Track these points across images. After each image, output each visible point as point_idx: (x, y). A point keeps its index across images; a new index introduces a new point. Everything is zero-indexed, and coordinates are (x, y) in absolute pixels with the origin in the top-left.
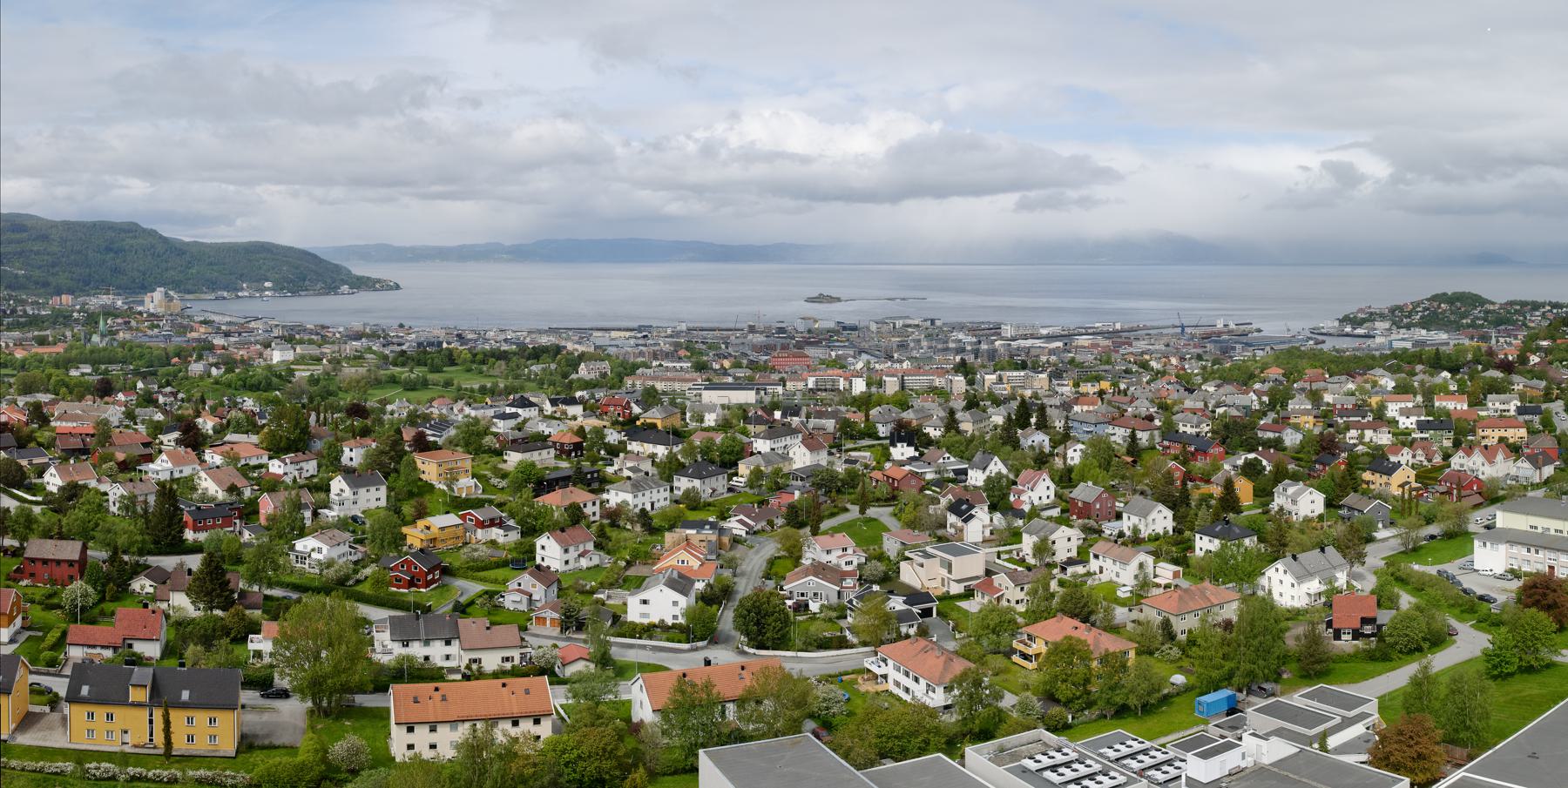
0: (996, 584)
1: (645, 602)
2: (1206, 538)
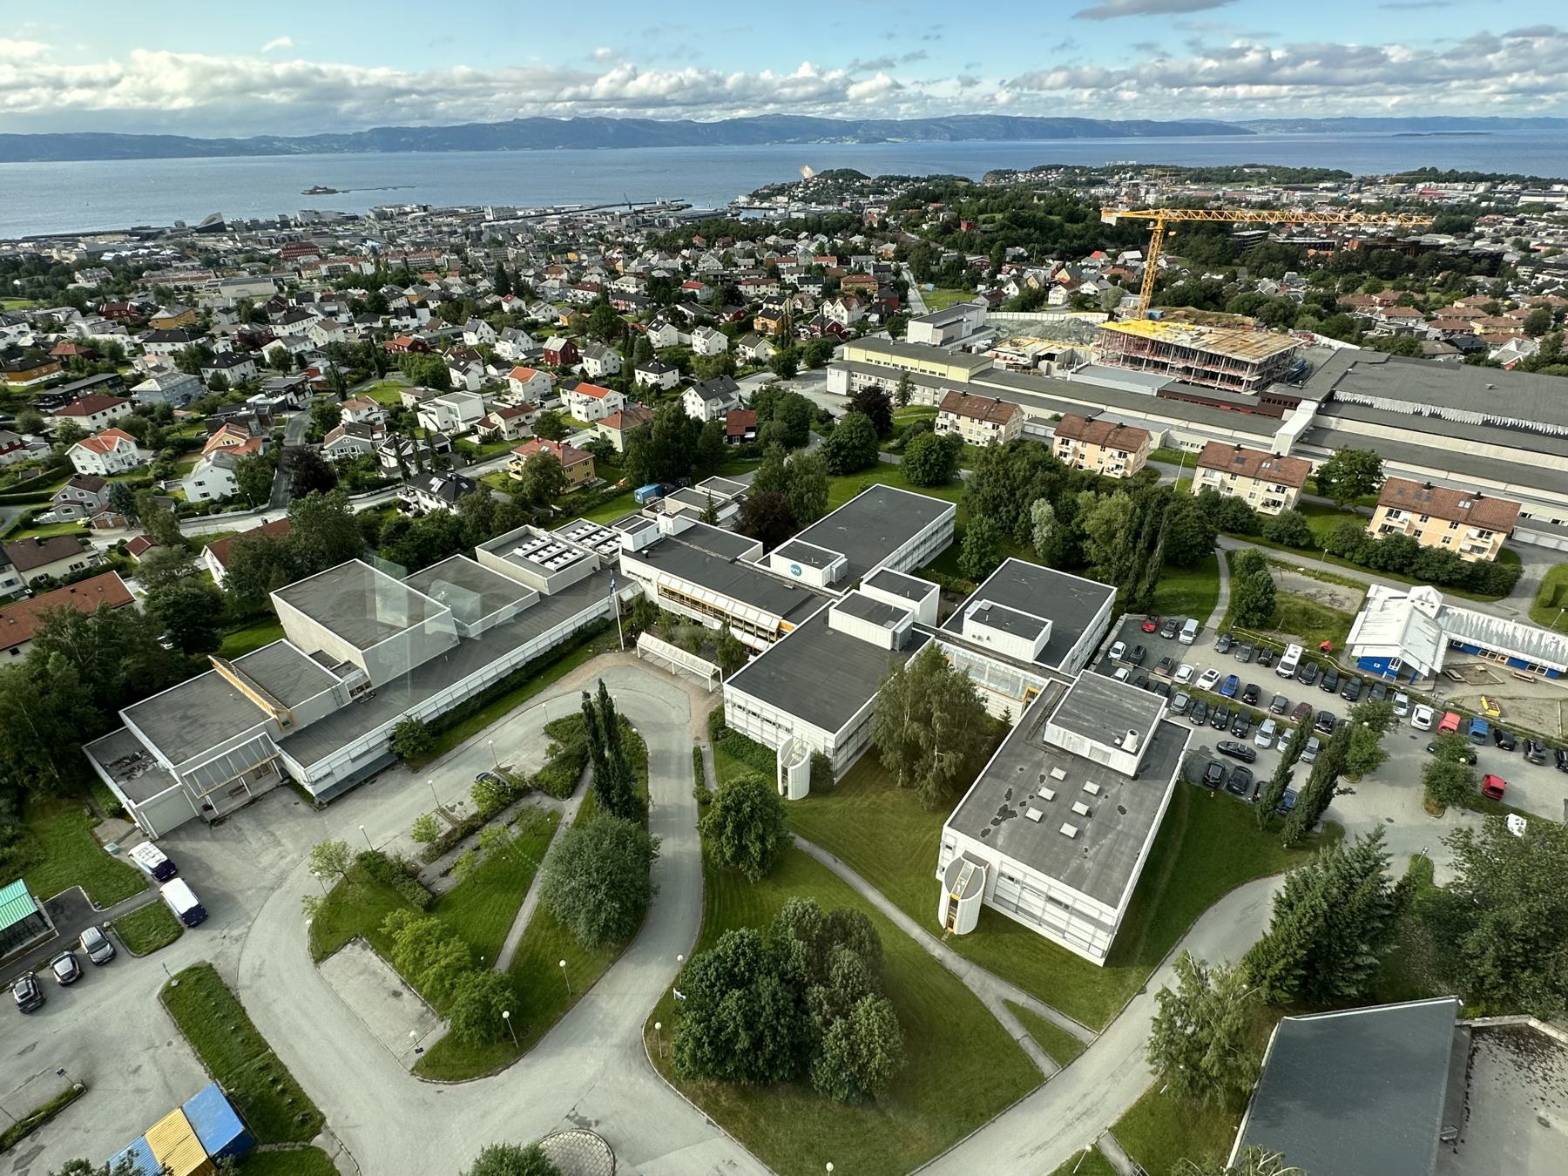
1: (200, 484)
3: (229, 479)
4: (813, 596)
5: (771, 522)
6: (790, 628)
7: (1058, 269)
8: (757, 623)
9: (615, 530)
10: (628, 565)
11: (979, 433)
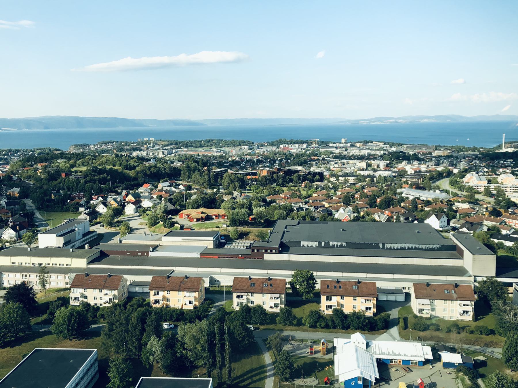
7: (127, 195)
11: (101, 299)
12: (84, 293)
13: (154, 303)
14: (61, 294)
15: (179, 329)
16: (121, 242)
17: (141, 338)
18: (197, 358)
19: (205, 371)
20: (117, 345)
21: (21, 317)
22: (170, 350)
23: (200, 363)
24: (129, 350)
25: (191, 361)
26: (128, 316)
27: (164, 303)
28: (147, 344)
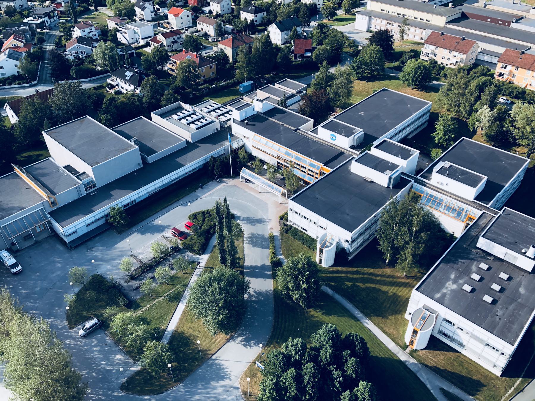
0: (158, 39)
2: (244, 13)
3: (16, 66)
4: (342, 153)
5: (319, 110)
6: (328, 170)
8: (310, 168)
9: (229, 108)
10: (237, 130)
11: (448, 59)
12: (435, 50)
13: (498, 76)
14: (414, 47)
15: (515, 106)
16: (485, 6)
17: (474, 104)
18: (523, 137)
19: (526, 150)
20: (451, 105)
21: (379, 59)
22: (498, 122)
23: (524, 142)
24: (459, 112)
25: (515, 138)
26: (469, 81)
27: (508, 78)
28: (478, 111)
